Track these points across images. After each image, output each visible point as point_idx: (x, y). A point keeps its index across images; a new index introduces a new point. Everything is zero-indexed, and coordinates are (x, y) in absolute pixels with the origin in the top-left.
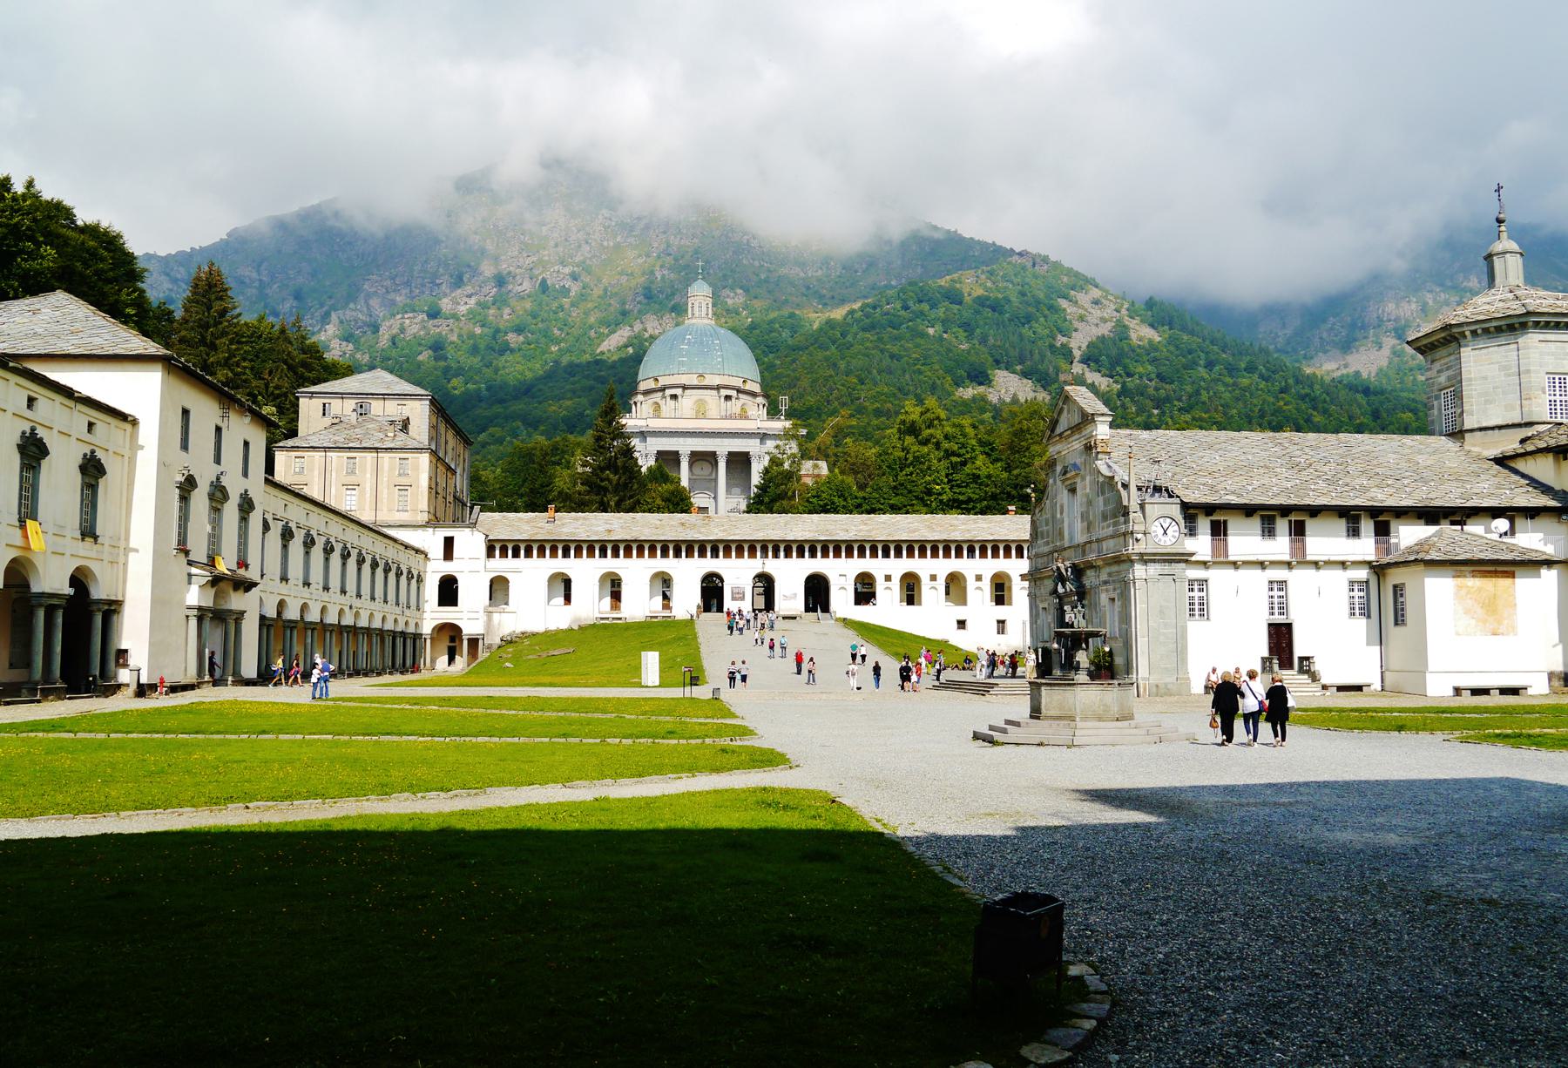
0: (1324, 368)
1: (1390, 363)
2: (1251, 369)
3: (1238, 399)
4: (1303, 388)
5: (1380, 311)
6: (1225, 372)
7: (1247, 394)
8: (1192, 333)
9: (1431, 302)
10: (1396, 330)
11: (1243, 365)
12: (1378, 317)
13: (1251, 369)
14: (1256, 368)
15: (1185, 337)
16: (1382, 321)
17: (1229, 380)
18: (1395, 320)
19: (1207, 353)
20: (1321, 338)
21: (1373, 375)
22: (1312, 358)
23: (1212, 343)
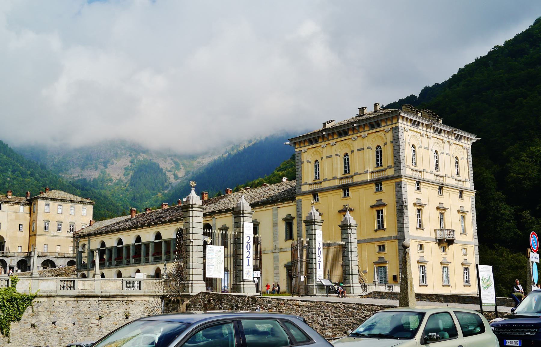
0: (72, 175)
1: (99, 176)
2: (32, 175)
3: (21, 188)
4: (52, 186)
5: (99, 154)
6: (20, 175)
7: (27, 186)
8: (8, 156)
9: (119, 152)
10: (104, 163)
11: (29, 172)
12: (98, 156)
13: (32, 175)
14: (34, 175)
15: (5, 157)
16: (99, 158)
17: (21, 179)
18: (104, 158)
19: (13, 166)
20: (73, 162)
21: (92, 180)
22: (68, 170)
23: (17, 161)
